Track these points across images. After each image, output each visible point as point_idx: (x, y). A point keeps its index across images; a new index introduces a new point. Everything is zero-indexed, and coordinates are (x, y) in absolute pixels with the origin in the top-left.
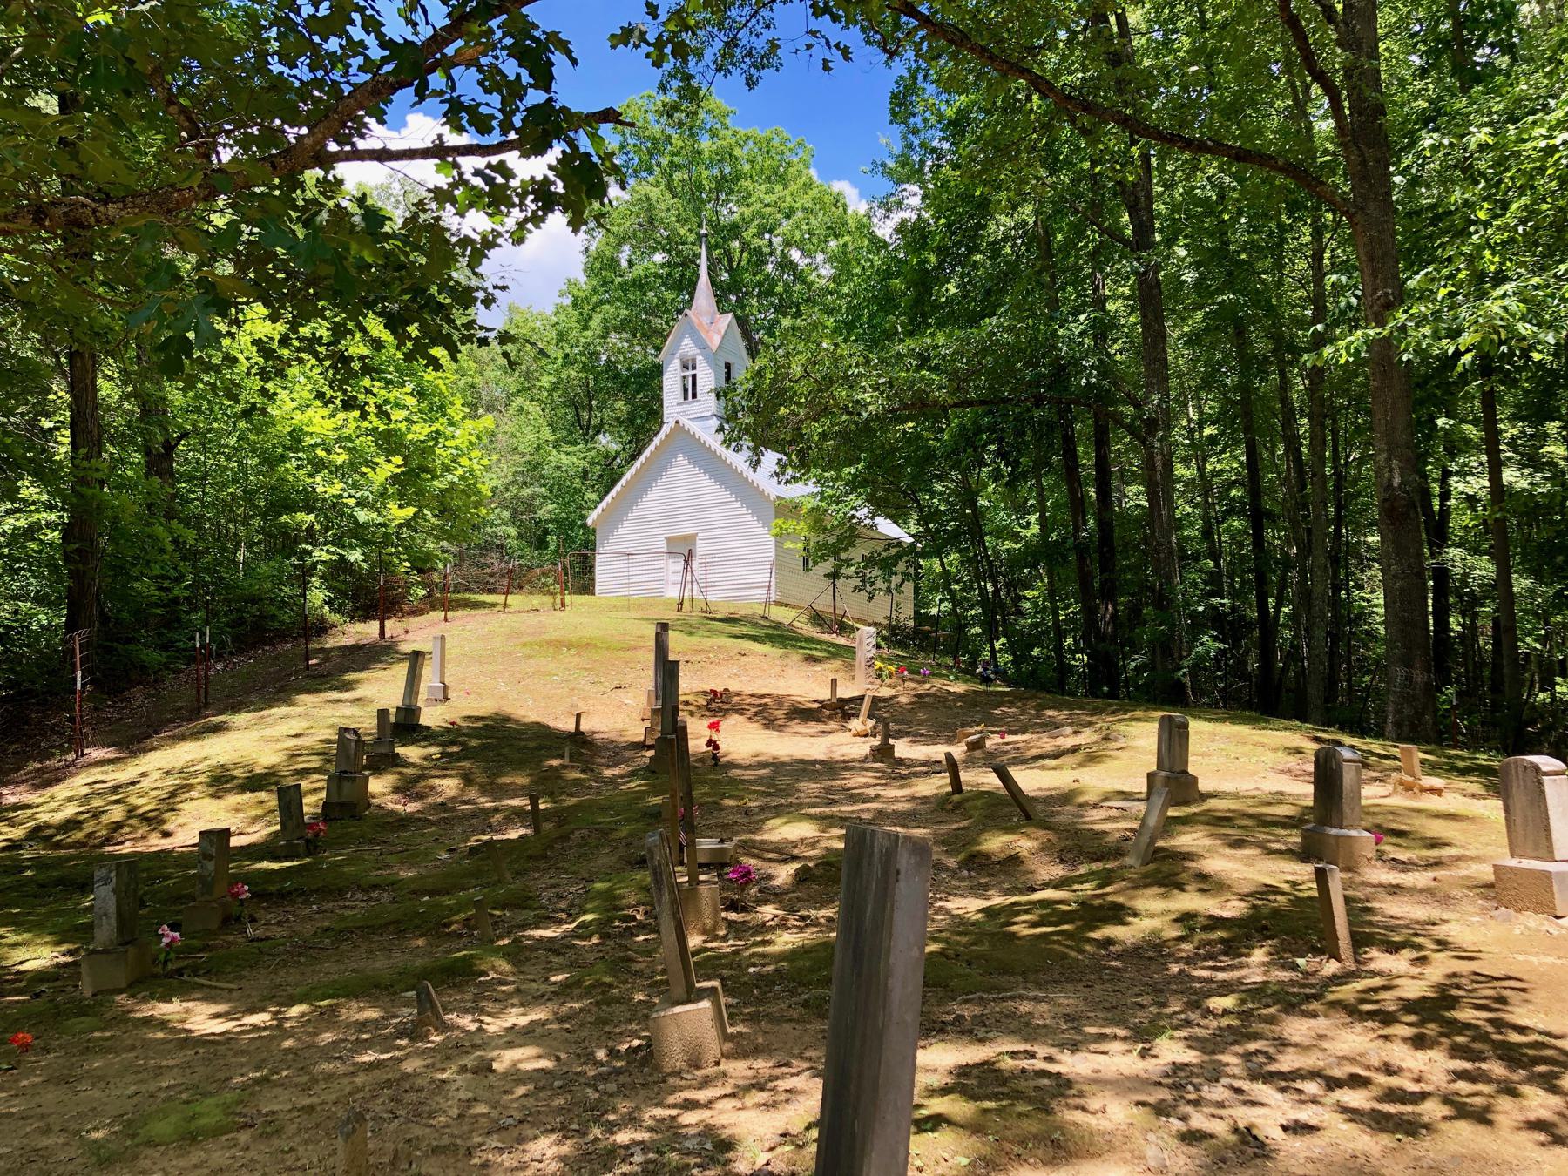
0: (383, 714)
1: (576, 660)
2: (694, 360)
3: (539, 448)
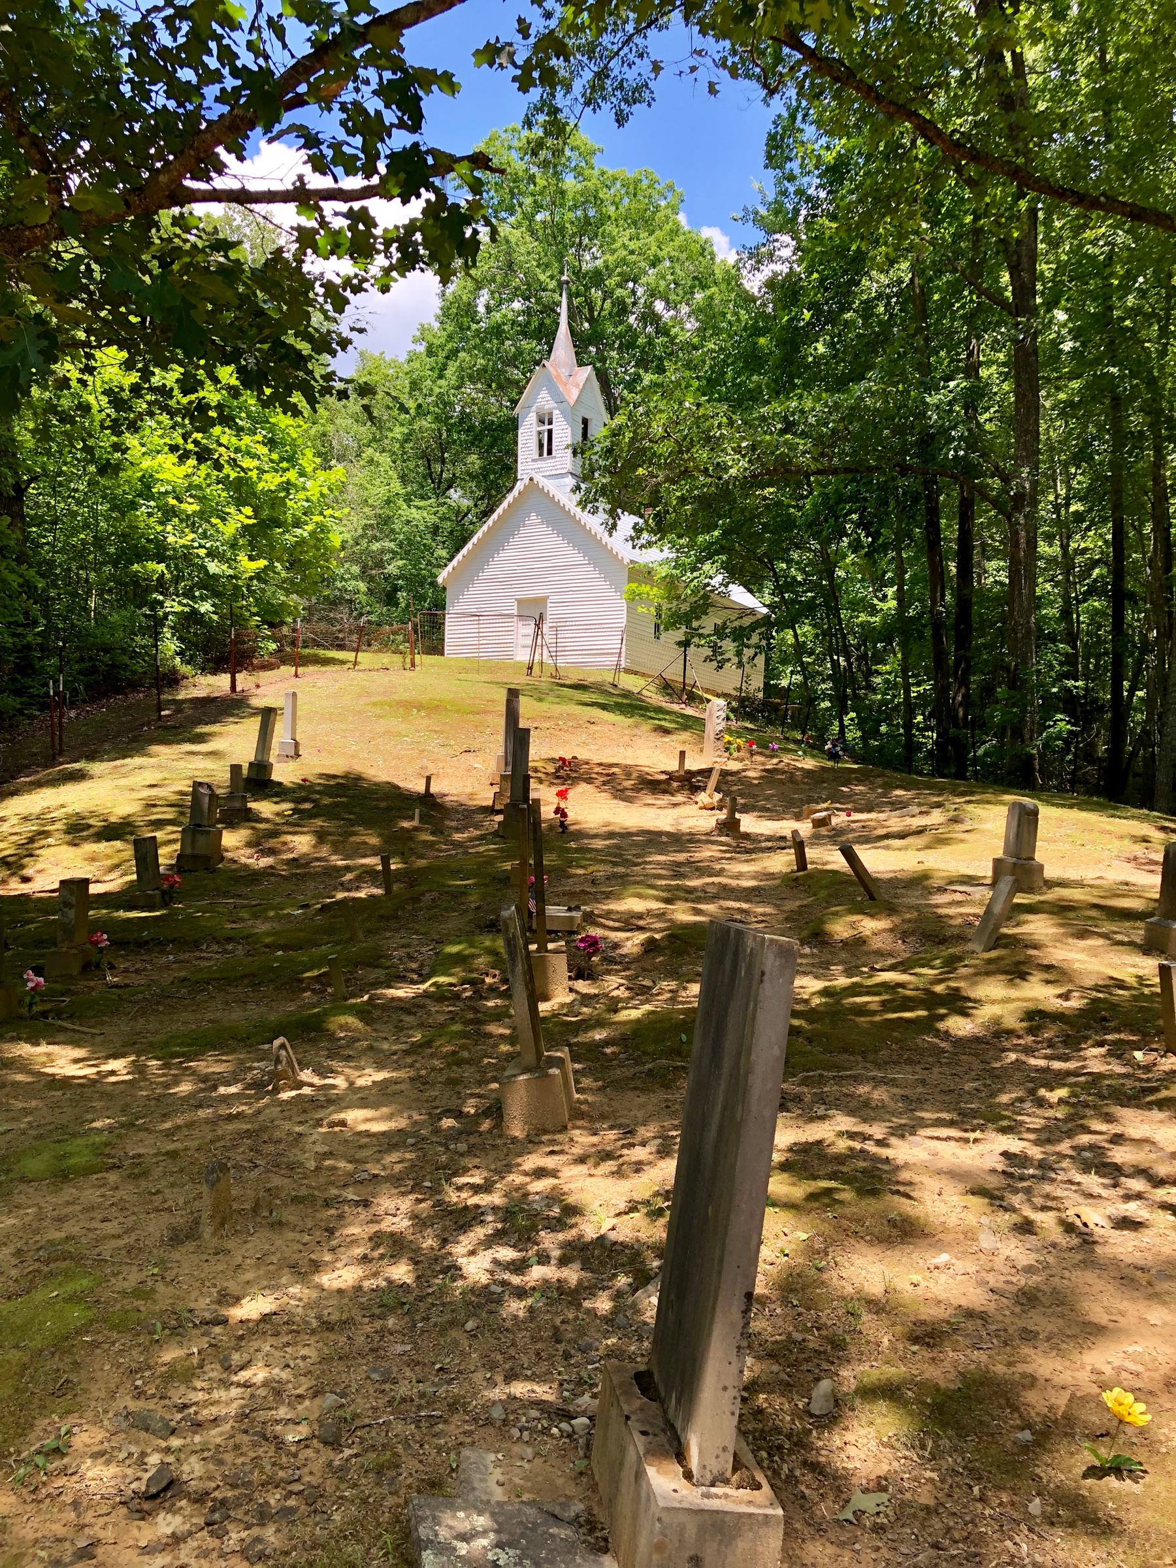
0: (235, 769)
1: (426, 721)
2: (551, 414)
3: (388, 502)
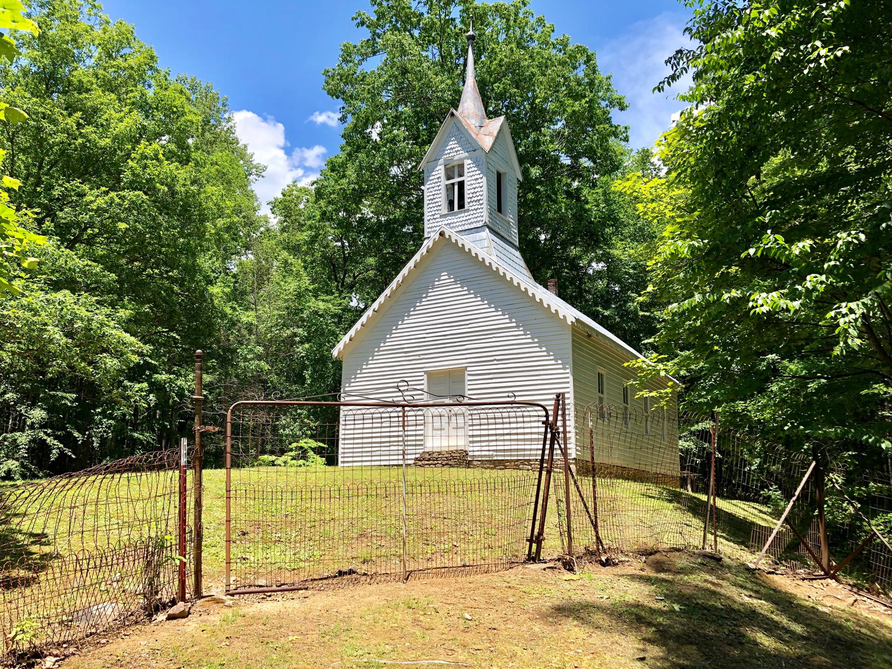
2: (461, 166)
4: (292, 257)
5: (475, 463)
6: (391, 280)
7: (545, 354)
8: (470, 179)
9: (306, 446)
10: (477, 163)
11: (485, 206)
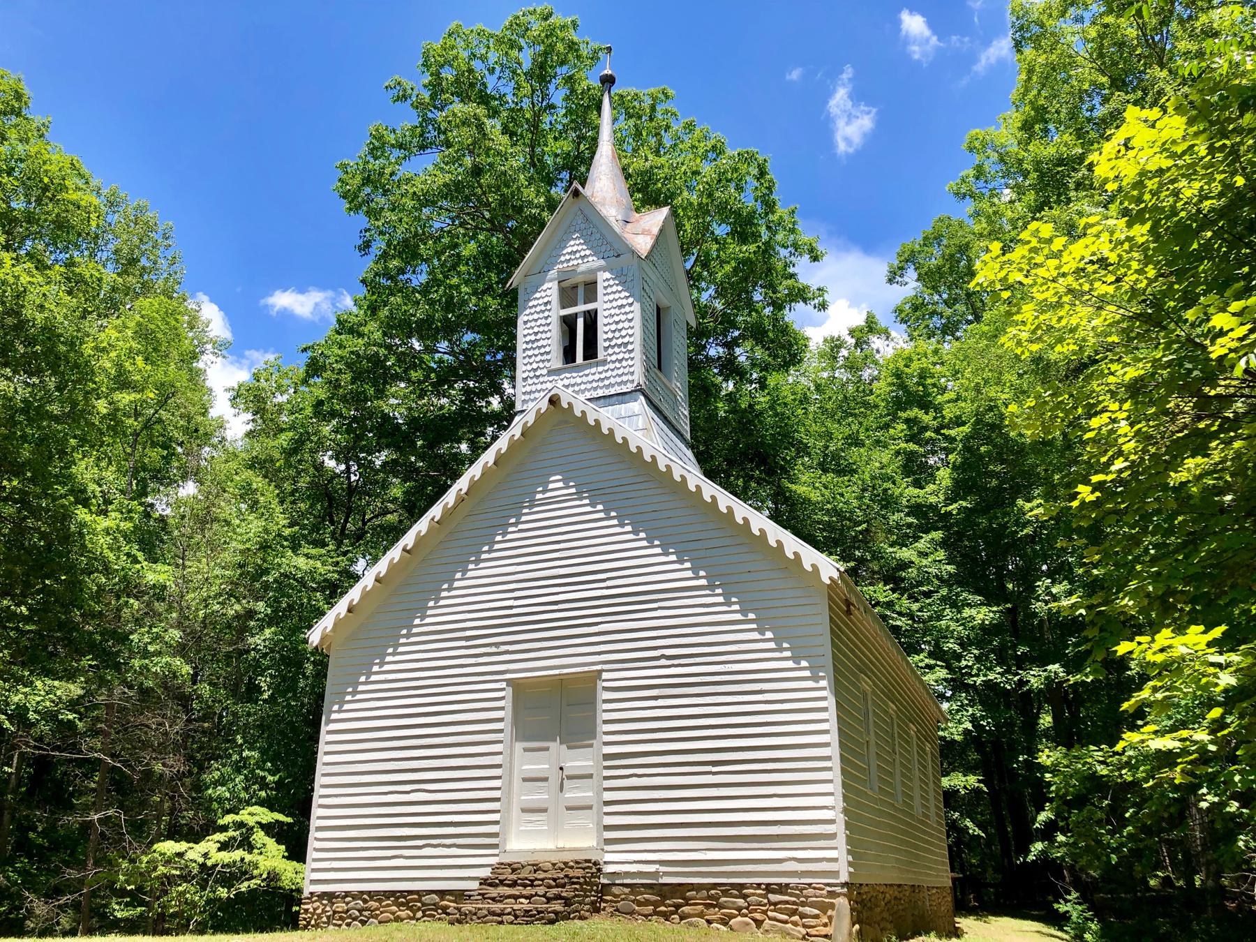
3: (264, 547)
4: (260, 479)
5: (615, 890)
6: (444, 489)
7: (772, 645)
8: (608, 305)
9: (251, 821)
10: (622, 277)
11: (638, 355)
